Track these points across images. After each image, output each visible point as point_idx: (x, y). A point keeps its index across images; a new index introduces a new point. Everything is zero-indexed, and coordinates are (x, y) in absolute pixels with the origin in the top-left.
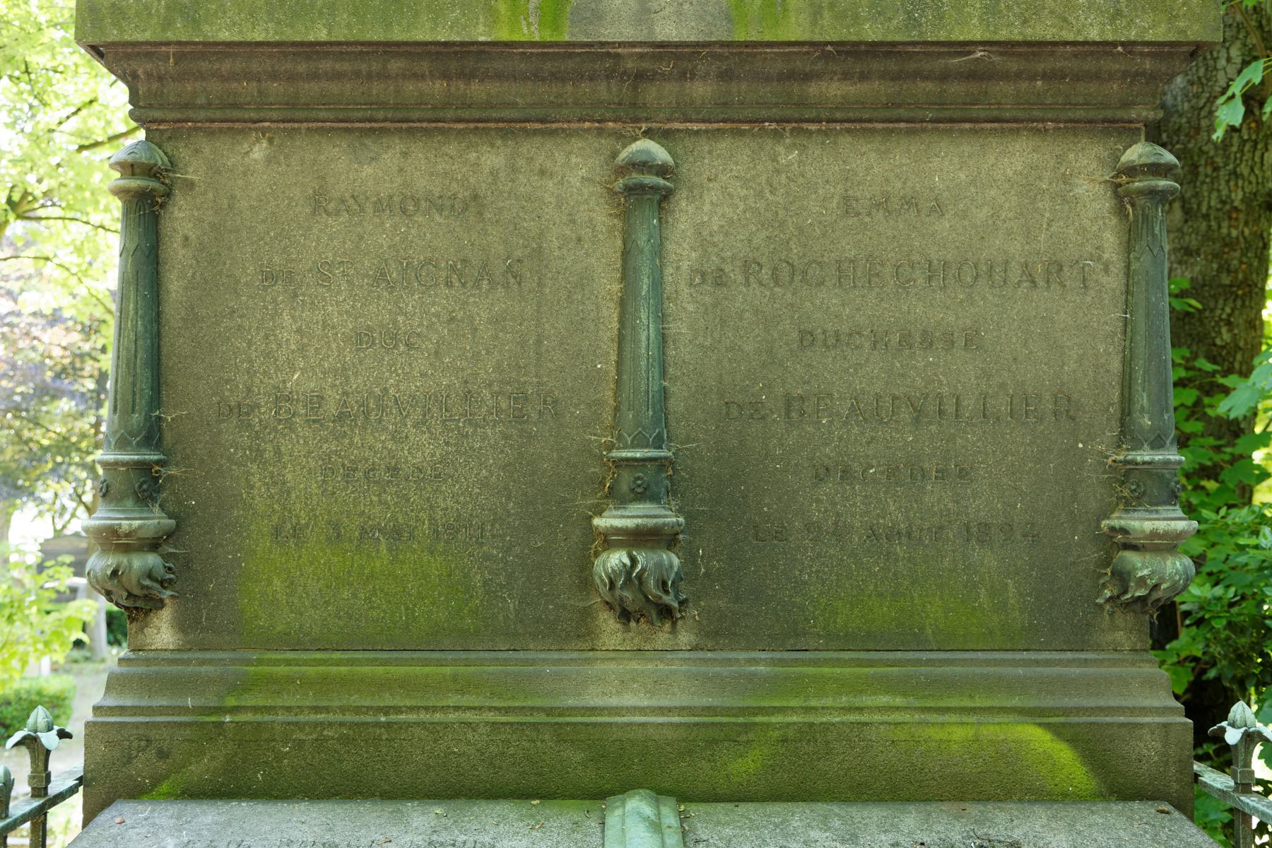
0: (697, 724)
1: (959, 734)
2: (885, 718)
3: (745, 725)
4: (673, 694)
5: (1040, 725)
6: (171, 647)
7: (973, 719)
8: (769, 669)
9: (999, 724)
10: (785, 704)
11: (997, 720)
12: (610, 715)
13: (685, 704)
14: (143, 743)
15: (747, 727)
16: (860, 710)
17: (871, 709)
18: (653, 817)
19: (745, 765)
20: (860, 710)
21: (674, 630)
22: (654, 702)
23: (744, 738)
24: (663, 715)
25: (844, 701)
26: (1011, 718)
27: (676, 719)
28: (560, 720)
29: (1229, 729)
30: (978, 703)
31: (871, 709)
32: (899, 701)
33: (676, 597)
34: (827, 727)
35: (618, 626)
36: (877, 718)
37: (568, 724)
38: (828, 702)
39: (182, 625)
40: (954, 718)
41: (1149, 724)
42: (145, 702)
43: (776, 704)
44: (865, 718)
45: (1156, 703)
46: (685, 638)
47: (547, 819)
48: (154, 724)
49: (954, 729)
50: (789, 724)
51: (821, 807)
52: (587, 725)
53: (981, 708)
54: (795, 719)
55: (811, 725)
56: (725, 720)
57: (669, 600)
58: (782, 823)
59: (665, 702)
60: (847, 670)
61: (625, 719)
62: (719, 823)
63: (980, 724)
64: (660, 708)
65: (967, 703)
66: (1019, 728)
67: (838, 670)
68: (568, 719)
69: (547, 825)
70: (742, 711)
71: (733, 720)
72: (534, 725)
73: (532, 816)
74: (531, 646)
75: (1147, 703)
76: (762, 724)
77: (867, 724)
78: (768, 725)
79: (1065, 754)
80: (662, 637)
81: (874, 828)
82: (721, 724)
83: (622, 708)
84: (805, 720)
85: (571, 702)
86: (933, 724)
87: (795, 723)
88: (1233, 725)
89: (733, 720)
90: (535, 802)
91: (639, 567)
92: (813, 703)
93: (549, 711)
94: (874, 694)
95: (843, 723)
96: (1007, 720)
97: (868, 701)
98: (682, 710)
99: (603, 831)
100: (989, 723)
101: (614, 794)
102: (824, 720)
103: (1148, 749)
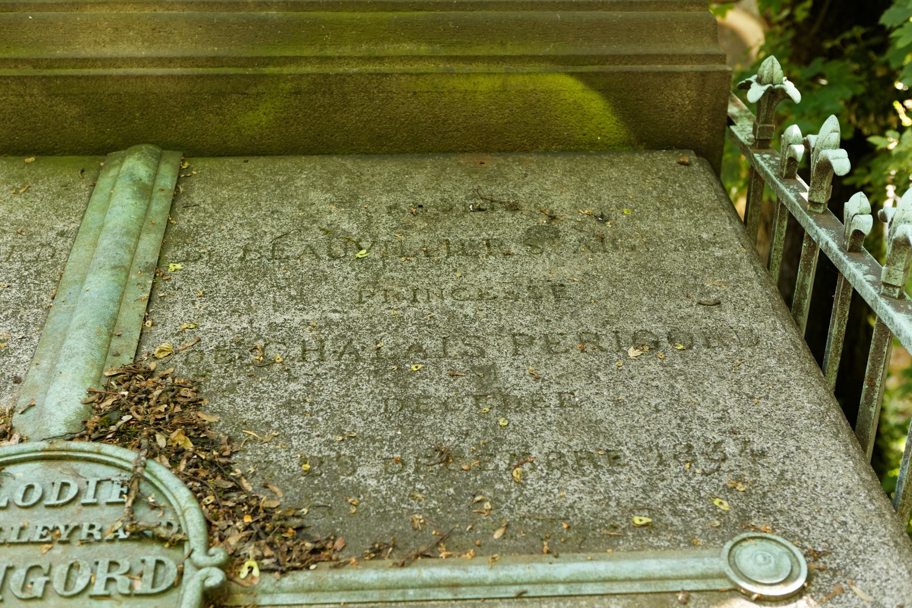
0: (200, 76)
1: (485, 84)
2: (408, 68)
3: (254, 76)
4: (174, 42)
5: (572, 74)
7: (502, 68)
8: (281, 14)
9: (529, 73)
10: (298, 53)
11: (527, 69)
12: (104, 66)
13: (187, 54)
15: (257, 79)
16: (380, 59)
17: (393, 59)
18: (146, 180)
19: (258, 118)
20: (380, 59)
22: (153, 52)
23: (253, 90)
24: (163, 66)
25: (364, 49)
26: (543, 66)
27: (178, 71)
28: (48, 72)
30: (510, 51)
31: (393, 59)
32: (424, 49)
34: (343, 78)
36: (399, 67)
37: (57, 77)
38: (347, 50)
40: (482, 67)
41: (686, 73)
43: (289, 53)
44: (385, 68)
45: (698, 50)
47: (36, 181)
49: (481, 79)
50: (302, 75)
51: (334, 162)
52: (79, 78)
53: (510, 57)
54: (309, 69)
55: (326, 76)
56: (232, 71)
58: (285, 182)
59: (165, 52)
60: (369, 15)
61: (121, 71)
62: (220, 183)
63: (508, 74)
64: (160, 59)
65: (498, 51)
66: (550, 78)
67: (358, 15)
68: (57, 72)
69: (35, 187)
70: (251, 61)
71: (241, 71)
72: (20, 79)
73: (21, 177)
75: (688, 50)
76: (273, 76)
77: (386, 75)
78: (279, 77)
79: (595, 105)
81: (378, 187)
82: (227, 76)
83: (117, 59)
84: (321, 71)
85: (59, 53)
86: (458, 74)
87: (308, 75)
88: (759, 81)
89: (241, 71)
90: (32, 159)
92: (330, 52)
93: (36, 63)
94: (398, 41)
95: (361, 74)
96: (537, 69)
97: (390, 49)
98: (184, 61)
99: (90, 196)
100: (518, 73)
101: (117, 149)
102: (341, 70)
103: (683, 99)
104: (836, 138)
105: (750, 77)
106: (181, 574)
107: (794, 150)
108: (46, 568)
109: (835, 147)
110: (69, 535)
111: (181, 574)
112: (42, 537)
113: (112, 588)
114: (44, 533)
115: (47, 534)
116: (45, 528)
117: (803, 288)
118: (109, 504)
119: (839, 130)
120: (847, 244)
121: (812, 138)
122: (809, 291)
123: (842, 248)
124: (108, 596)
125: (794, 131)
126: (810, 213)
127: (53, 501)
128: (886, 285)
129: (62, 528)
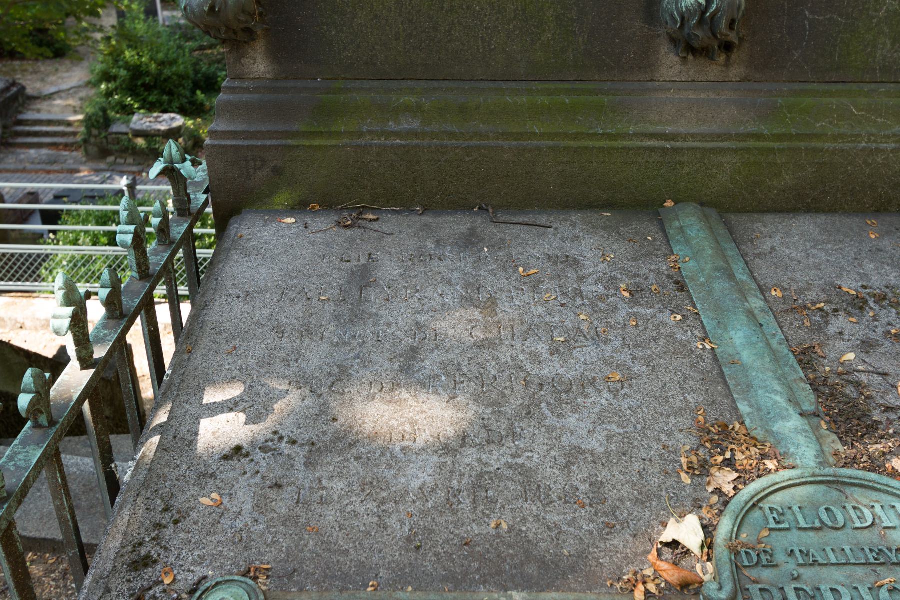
6: (268, 76)
14: (259, 163)
21: (727, 64)
33: (738, 34)
35: (677, 59)
39: (275, 54)
42: (254, 128)
46: (736, 72)
48: (265, 147)
57: (733, 37)
74: (597, 77)
80: (713, 71)
91: (715, 6)
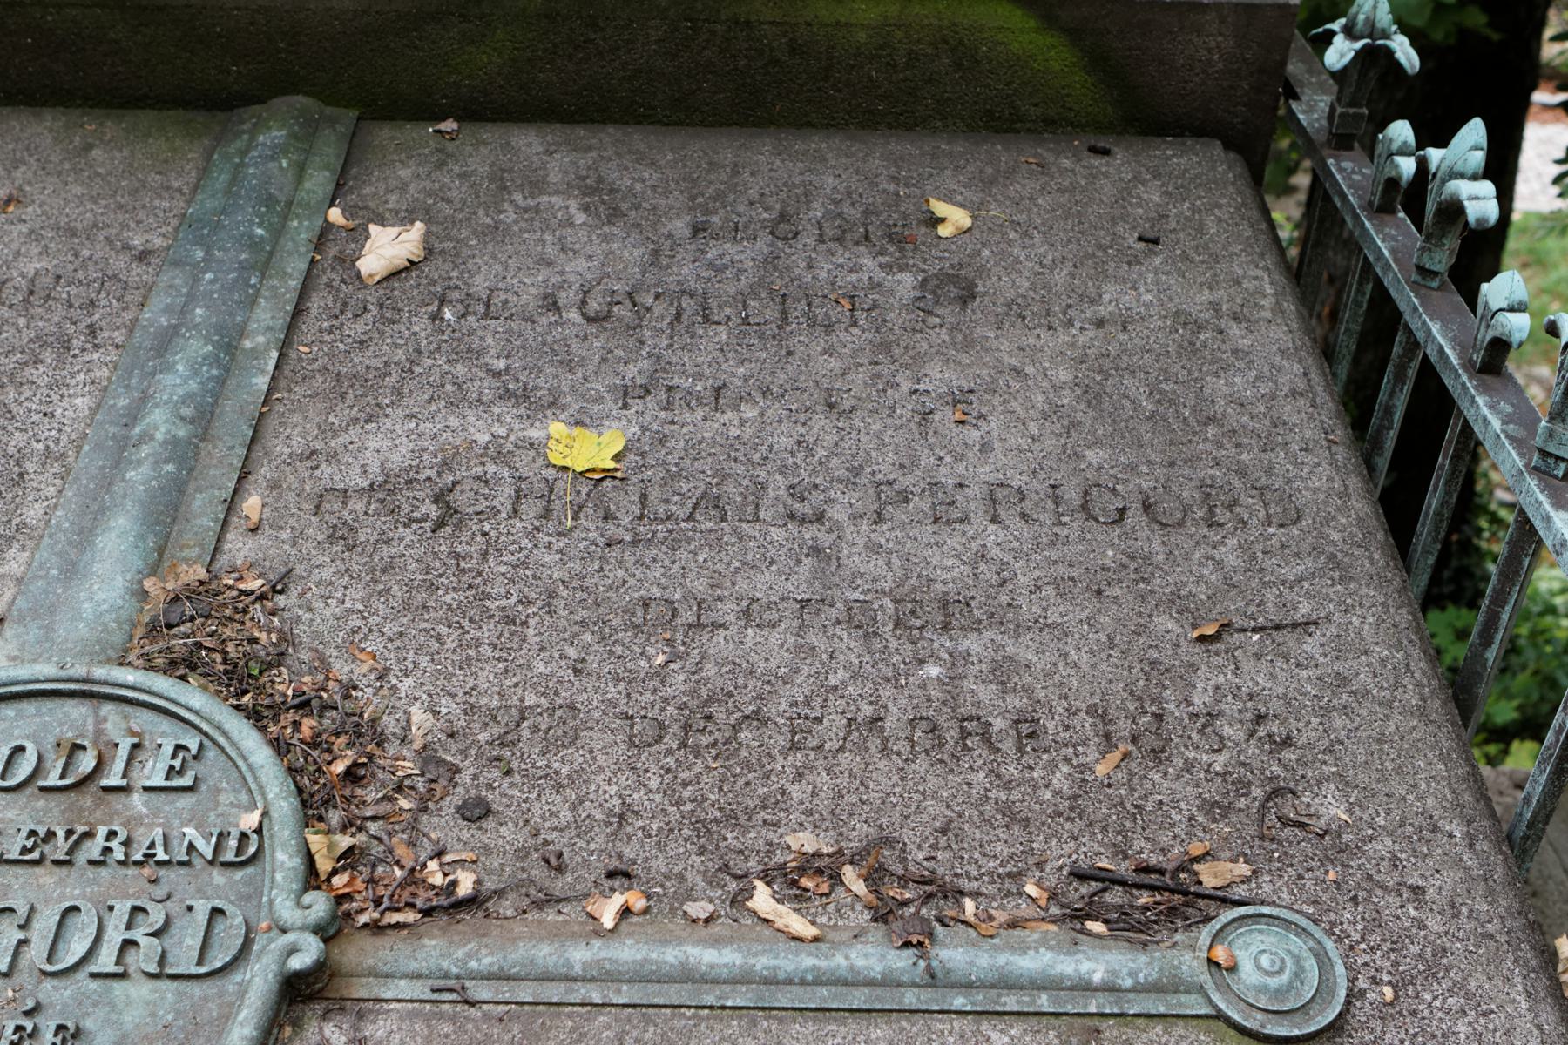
29: (1339, 40)
88: (1350, 32)
103: (1209, 50)
104: (1478, 159)
105: (1333, 20)
106: (247, 943)
107: (1397, 166)
108: (22, 911)
109: (1474, 178)
110: (70, 852)
111: (247, 943)
112: (24, 850)
113: (131, 957)
114: (29, 844)
115: (35, 846)
116: (33, 833)
117: (1388, 411)
118: (146, 789)
119: (1485, 145)
120: (1478, 357)
121: (1435, 155)
122: (1398, 417)
123: (1468, 365)
124: (123, 976)
125: (1401, 131)
126: (1415, 286)
127: (53, 780)
128: (1545, 454)
129: (61, 834)
